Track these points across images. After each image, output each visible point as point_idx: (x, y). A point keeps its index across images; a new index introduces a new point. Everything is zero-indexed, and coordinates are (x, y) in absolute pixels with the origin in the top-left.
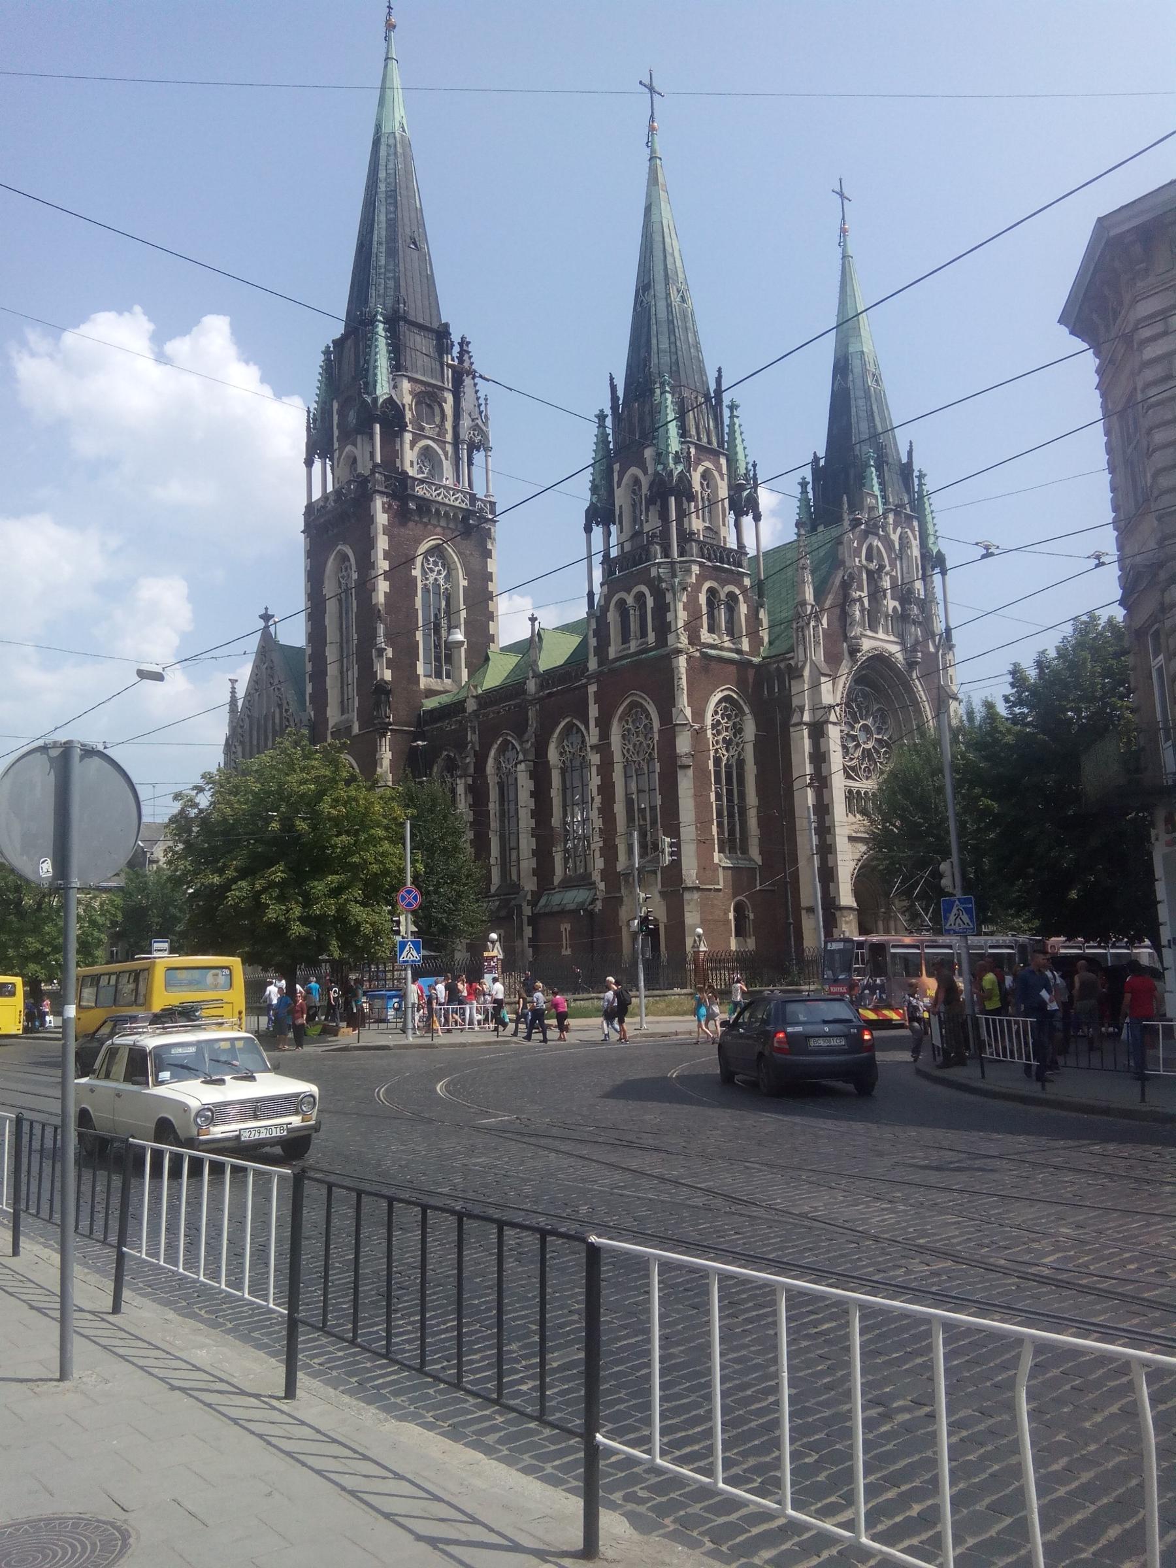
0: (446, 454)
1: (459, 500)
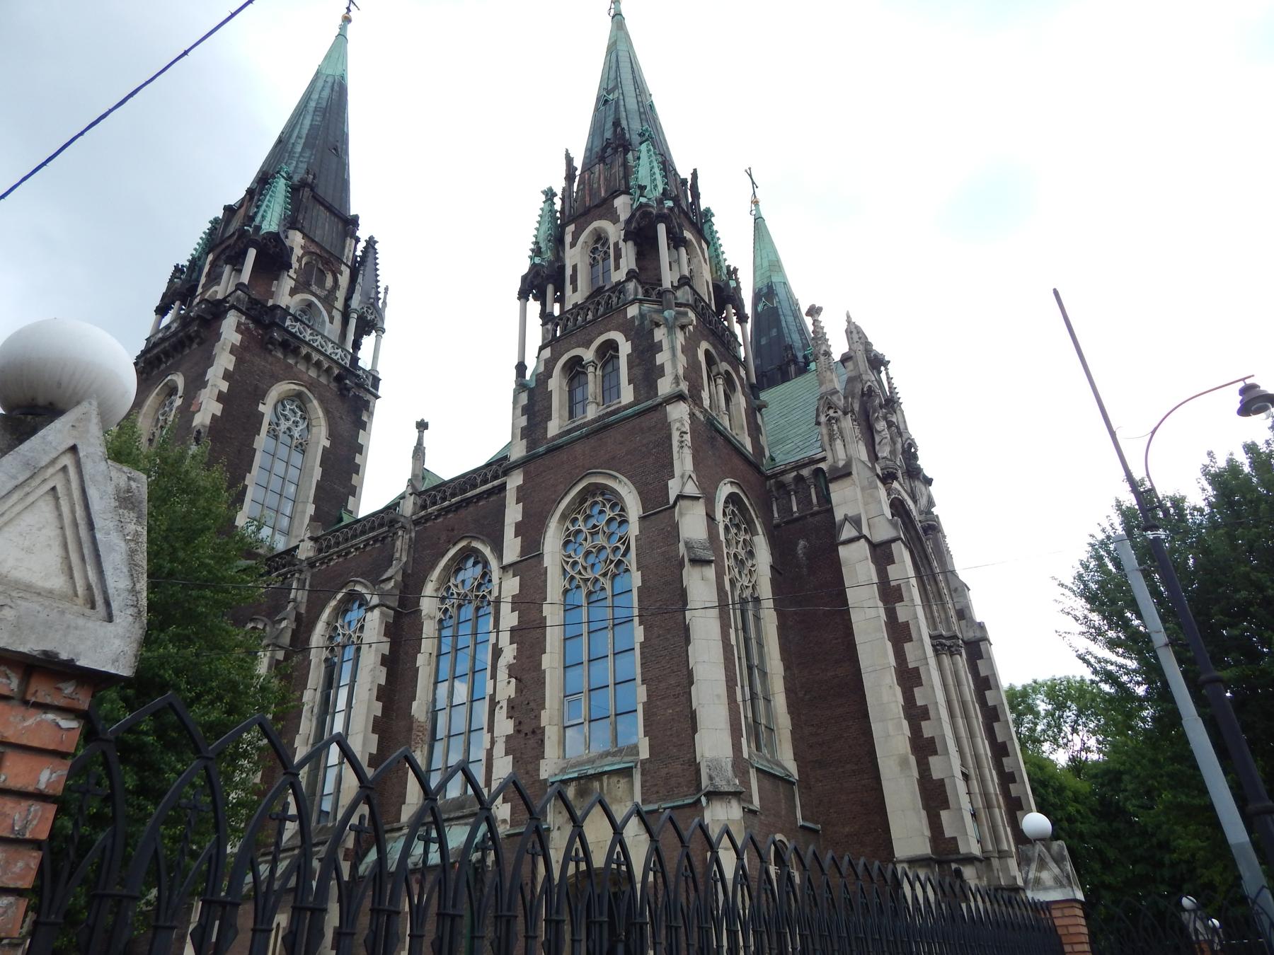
0: (332, 319)
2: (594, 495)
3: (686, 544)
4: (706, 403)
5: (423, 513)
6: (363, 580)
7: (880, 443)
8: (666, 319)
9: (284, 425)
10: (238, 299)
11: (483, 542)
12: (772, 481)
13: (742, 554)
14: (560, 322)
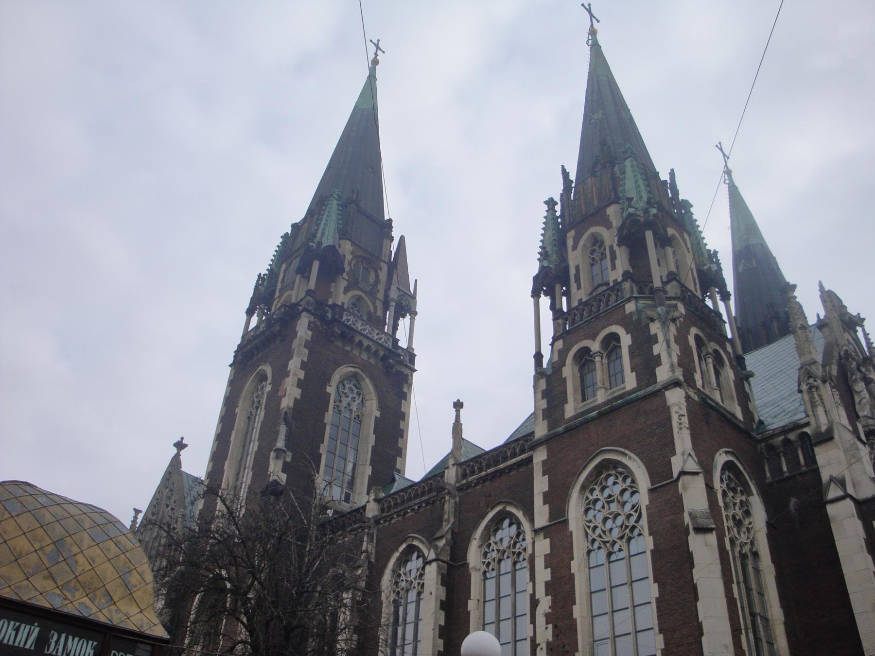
1: (383, 340)
2: (608, 469)
3: (690, 514)
4: (699, 384)
5: (464, 481)
6: (419, 536)
7: (860, 403)
8: (659, 315)
9: (345, 401)
10: (308, 303)
11: (516, 507)
12: (763, 444)
13: (739, 513)
14: (568, 317)
